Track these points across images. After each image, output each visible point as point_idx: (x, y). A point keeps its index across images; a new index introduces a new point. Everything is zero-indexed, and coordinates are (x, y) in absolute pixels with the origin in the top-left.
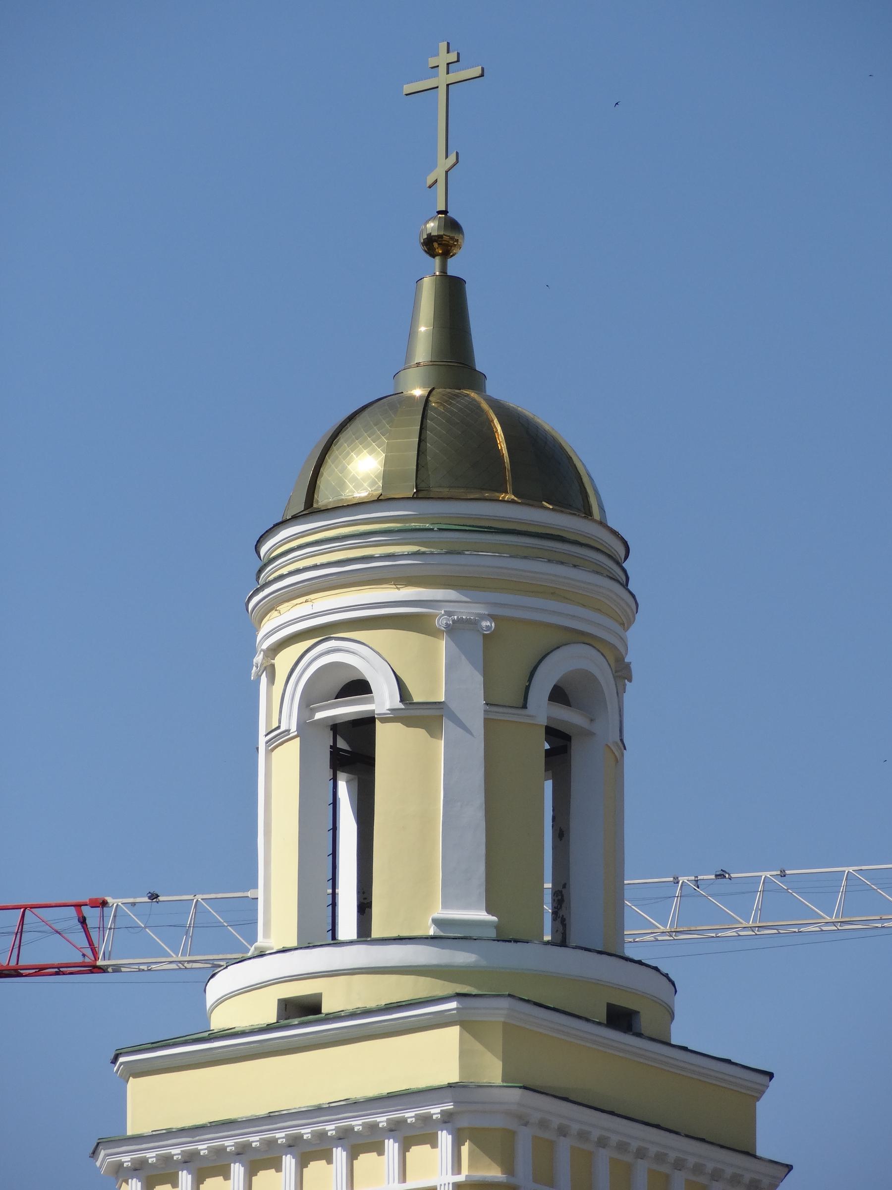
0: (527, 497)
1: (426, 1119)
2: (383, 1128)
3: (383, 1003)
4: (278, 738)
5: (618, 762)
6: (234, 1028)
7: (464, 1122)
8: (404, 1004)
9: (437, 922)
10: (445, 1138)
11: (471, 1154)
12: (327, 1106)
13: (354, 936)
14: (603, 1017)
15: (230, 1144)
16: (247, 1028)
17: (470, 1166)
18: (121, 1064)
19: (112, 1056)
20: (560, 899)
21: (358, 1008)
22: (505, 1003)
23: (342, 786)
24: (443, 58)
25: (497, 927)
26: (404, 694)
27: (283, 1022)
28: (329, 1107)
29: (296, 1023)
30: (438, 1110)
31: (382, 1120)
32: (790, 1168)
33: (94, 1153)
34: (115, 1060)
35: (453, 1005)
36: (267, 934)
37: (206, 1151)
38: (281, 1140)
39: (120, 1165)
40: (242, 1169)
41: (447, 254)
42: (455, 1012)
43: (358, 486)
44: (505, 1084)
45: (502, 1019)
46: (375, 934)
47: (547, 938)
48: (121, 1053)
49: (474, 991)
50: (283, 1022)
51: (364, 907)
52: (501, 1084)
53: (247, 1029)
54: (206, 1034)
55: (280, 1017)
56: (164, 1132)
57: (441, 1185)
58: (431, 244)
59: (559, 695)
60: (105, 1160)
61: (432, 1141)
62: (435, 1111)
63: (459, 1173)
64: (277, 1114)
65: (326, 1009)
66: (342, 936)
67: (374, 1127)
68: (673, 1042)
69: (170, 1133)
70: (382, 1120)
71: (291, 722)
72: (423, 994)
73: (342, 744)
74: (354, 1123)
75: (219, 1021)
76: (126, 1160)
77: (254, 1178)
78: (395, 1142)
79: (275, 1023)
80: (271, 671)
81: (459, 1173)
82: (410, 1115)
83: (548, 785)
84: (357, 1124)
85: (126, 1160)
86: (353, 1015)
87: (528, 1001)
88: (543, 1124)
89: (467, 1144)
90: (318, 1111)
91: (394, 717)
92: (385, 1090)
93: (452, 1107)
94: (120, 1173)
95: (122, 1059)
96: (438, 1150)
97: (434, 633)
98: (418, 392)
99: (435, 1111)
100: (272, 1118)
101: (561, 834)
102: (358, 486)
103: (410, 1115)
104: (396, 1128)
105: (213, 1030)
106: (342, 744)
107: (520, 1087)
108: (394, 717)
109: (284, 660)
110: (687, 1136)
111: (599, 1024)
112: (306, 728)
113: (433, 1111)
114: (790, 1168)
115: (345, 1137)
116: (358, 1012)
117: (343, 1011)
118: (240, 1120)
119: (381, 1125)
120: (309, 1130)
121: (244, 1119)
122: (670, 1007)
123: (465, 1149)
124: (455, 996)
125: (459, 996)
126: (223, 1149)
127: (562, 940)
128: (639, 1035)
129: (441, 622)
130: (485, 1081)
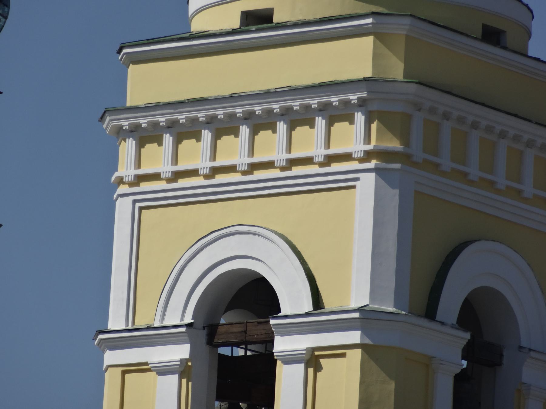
2: (314, 108)
3: (318, 17)
6: (208, 31)
8: (333, 18)
12: (274, 91)
14: (479, 35)
16: (219, 31)
18: (124, 54)
19: (118, 49)
21: (300, 20)
22: (407, 21)
27: (244, 28)
28: (276, 92)
29: (254, 29)
30: (355, 97)
34: (119, 51)
37: (184, 120)
38: (239, 114)
40: (210, 134)
42: (371, 26)
44: (405, 80)
45: (405, 33)
48: (124, 47)
49: (385, 11)
50: (244, 28)
52: (403, 80)
53: (218, 32)
54: (187, 35)
55: (242, 24)
56: (154, 105)
57: (355, 152)
61: (351, 120)
63: (369, 143)
64: (237, 95)
68: (530, 54)
74: (293, 104)
77: (218, 141)
78: (323, 118)
79: (239, 29)
81: (369, 143)
87: (424, 20)
88: (432, 111)
89: (375, 123)
92: (317, 81)
93: (366, 95)
95: (125, 51)
96: (355, 126)
100: (233, 98)
105: (193, 32)
107: (416, 83)
110: (537, 123)
111: (476, 39)
113: (351, 98)
115: (286, 113)
116: (300, 23)
117: (288, 22)
118: (210, 98)
119: (313, 106)
120: (260, 108)
121: (213, 98)
122: (528, 28)
124: (371, 14)
130: (390, 77)
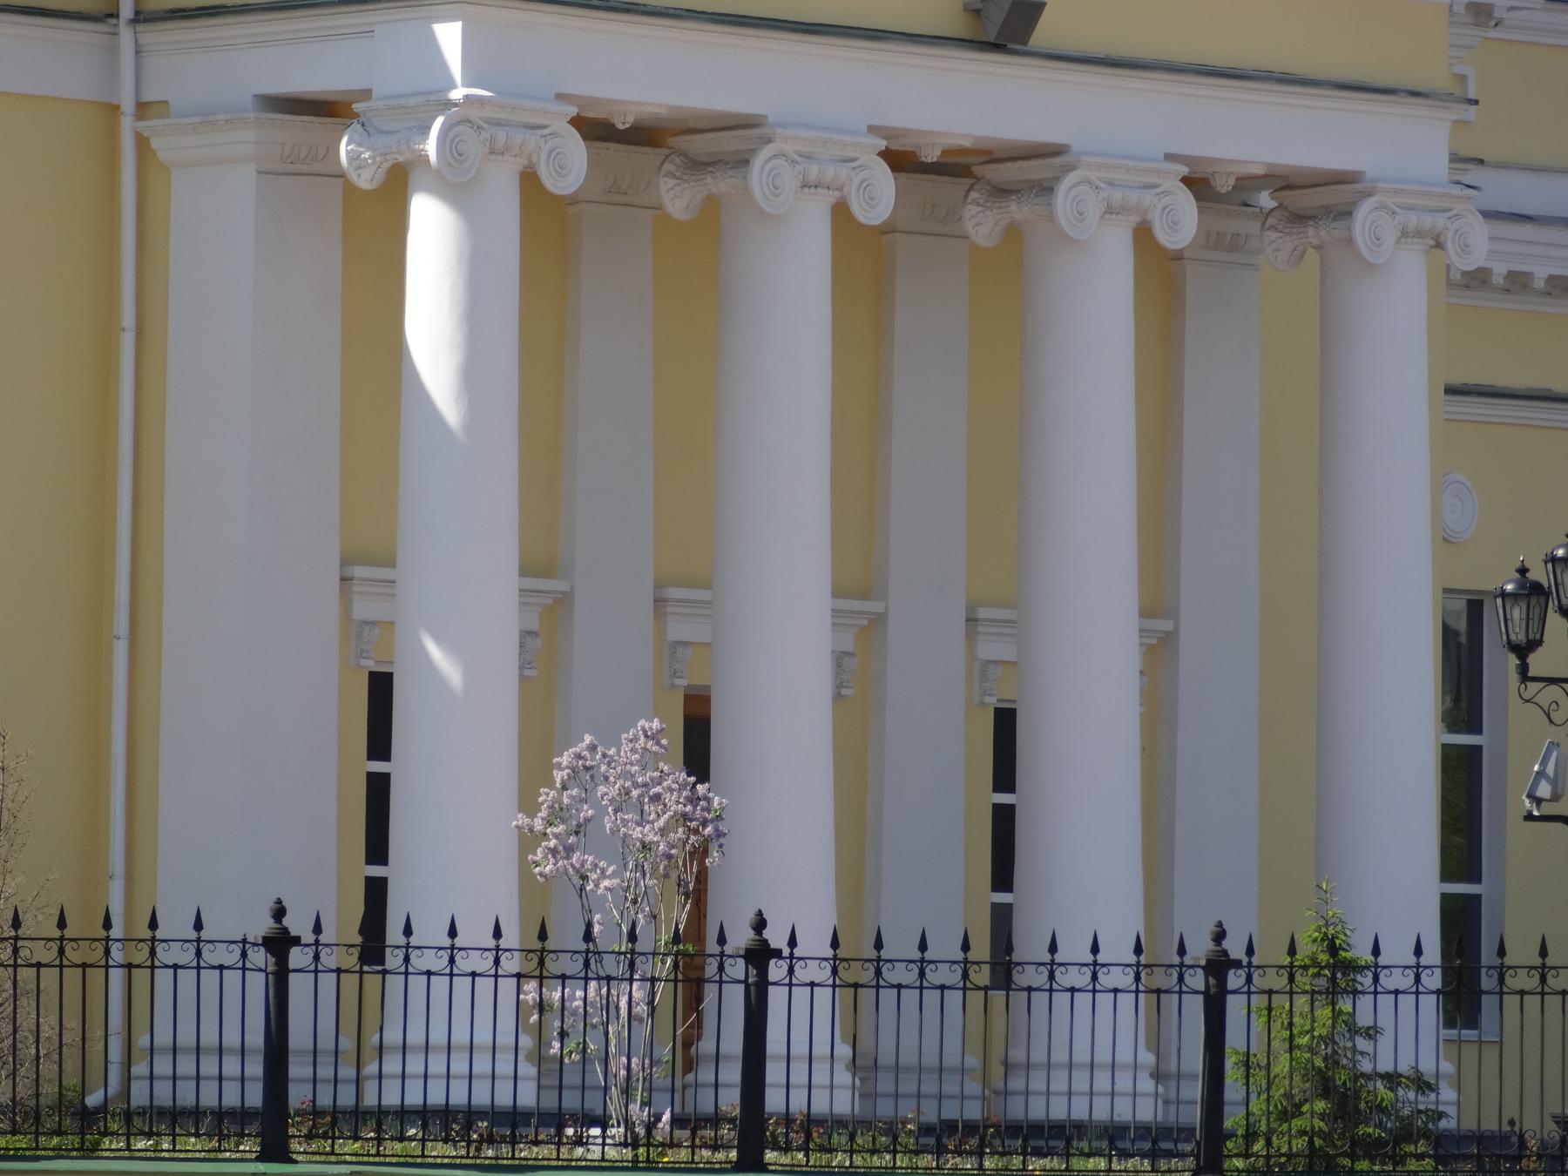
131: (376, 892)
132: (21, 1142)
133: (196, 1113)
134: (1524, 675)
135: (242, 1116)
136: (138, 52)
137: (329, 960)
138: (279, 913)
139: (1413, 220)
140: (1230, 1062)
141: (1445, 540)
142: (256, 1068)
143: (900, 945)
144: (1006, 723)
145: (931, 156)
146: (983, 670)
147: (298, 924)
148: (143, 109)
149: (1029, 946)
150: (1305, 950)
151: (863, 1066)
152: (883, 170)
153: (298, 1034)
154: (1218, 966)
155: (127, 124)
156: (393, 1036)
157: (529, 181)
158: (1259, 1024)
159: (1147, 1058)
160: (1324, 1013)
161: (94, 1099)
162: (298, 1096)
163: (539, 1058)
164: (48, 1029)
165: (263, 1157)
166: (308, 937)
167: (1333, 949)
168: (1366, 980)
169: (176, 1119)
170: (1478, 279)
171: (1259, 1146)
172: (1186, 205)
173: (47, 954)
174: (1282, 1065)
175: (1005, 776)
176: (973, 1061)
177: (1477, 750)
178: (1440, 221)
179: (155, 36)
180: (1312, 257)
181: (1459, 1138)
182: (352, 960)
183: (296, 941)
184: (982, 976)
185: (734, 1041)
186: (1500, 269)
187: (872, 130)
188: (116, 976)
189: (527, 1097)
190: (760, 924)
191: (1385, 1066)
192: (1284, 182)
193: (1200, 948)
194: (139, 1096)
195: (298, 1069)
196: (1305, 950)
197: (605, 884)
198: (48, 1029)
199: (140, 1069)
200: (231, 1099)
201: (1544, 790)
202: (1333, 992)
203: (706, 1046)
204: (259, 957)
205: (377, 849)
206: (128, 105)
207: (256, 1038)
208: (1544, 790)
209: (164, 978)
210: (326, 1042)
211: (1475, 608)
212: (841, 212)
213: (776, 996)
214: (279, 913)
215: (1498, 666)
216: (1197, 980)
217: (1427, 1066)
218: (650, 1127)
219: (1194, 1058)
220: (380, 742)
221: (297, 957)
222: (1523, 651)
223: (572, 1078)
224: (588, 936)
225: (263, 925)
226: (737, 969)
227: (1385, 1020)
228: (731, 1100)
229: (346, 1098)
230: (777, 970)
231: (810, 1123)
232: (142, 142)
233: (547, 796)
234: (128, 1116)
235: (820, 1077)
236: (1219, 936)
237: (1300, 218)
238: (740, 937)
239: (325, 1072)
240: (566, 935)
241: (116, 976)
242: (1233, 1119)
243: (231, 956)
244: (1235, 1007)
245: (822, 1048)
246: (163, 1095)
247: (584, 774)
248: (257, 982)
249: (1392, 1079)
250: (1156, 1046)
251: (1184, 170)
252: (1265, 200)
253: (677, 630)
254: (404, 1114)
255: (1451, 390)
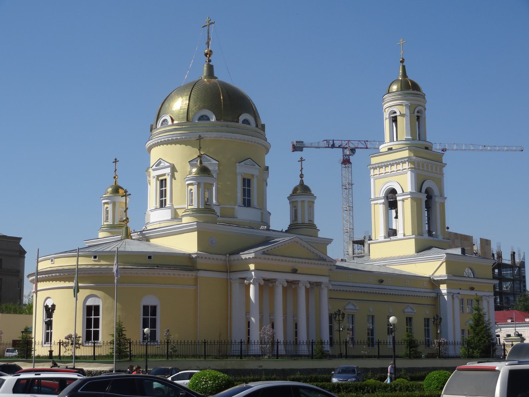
0: (413, 90)
1: (405, 161)
4: (386, 119)
5: (425, 119)
7: (409, 161)
9: (405, 138)
10: (407, 163)
11: (410, 164)
13: (396, 141)
15: (383, 165)
17: (410, 165)
20: (419, 135)
23: (394, 124)
24: (401, 40)
25: (412, 139)
26: (400, 113)
31: (400, 161)
32: (446, 164)
33: (368, 166)
35: (407, 148)
36: (386, 141)
39: (371, 167)
41: (403, 63)
43: (394, 90)
46: (398, 140)
47: (418, 139)
51: (397, 137)
58: (401, 62)
59: (418, 112)
60: (369, 167)
62: (406, 160)
65: (393, 149)
66: (394, 141)
67: (399, 162)
69: (376, 164)
70: (400, 161)
71: (388, 117)
72: (404, 147)
73: (393, 119)
75: (381, 151)
76: (371, 167)
80: (385, 111)
82: (403, 160)
83: (417, 122)
84: (397, 162)
85: (371, 167)
86: (396, 149)
90: (393, 160)
91: (399, 116)
94: (371, 168)
97: (404, 106)
98: (400, 79)
99: (406, 160)
101: (419, 128)
102: (394, 90)
103: (403, 160)
104: (402, 162)
106: (393, 119)
108: (399, 116)
109: (386, 110)
112: (389, 117)
114: (446, 164)
123: (409, 164)
125: (408, 147)
126: (382, 165)
127: (419, 140)
128: (429, 150)
129: (404, 105)
131: (249, 338)
132: (222, 358)
133: (235, 355)
134: (335, 320)
135: (239, 355)
136: (230, 274)
137: (245, 343)
138: (241, 340)
139: (326, 285)
140: (314, 350)
141: (329, 310)
142: (240, 352)
143: (288, 341)
144: (296, 324)
145: (290, 281)
146: (294, 320)
147: (243, 341)
148: (230, 279)
149: (298, 341)
150: (319, 341)
151: (286, 351)
152: (286, 282)
153: (243, 349)
154: (313, 343)
155: (229, 280)
156: (250, 349)
157: (259, 284)
158: (316, 347)
159: (307, 349)
160: (321, 346)
161: (227, 354)
162: (243, 354)
163: (261, 350)
164: (224, 349)
165: (240, 359)
166: (243, 342)
167: (321, 341)
168: (324, 343)
169: (233, 356)
170: (331, 290)
171: (316, 356)
172: (309, 285)
173: (224, 344)
174: (317, 350)
175: (296, 328)
176: (294, 350)
177: (332, 325)
178: (328, 286)
179: (231, 273)
180: (318, 288)
181: (331, 355)
182: (247, 344)
183: (243, 342)
184: (295, 344)
185: (276, 349)
186: (333, 289)
187: (285, 279)
188: (229, 345)
189: (260, 354)
190: (278, 340)
191: (325, 350)
192: (316, 283)
193: (311, 341)
194: (231, 354)
195: (243, 352)
196: (319, 341)
197: (266, 337)
198: (224, 349)
199: (231, 352)
200: (238, 354)
201: (337, 329)
202: (321, 344)
203: (274, 349)
204: (240, 343)
205: (249, 335)
206: (229, 278)
207: (240, 349)
208: (337, 329)
209: (233, 345)
210: (245, 350)
211: (331, 314)
212: (283, 286)
213: (279, 346)
214: (241, 340)
215: (333, 319)
216: (311, 344)
217: (328, 350)
218: (270, 356)
219: (311, 349)
220: (249, 327)
221: (243, 343)
222: (335, 318)
223: (264, 352)
224: (265, 341)
225: (240, 341)
226: (276, 344)
227: (325, 347)
228: (276, 353)
229: (247, 354)
230: (279, 344)
231: (282, 355)
232: (230, 281)
233: (262, 330)
234: (230, 356)
235: (283, 351)
236: (313, 340)
237: (317, 285)
238: (276, 341)
239: (245, 352)
240: (263, 341)
241: (229, 345)
242: (314, 354)
243: (238, 343)
244: (314, 346)
245: (283, 349)
246: (233, 354)
247: (265, 329)
248: (240, 345)
249: (326, 351)
250: (308, 349)
251: (309, 282)
252: (315, 284)
253: (271, 318)
254: (251, 355)
255: (329, 298)
